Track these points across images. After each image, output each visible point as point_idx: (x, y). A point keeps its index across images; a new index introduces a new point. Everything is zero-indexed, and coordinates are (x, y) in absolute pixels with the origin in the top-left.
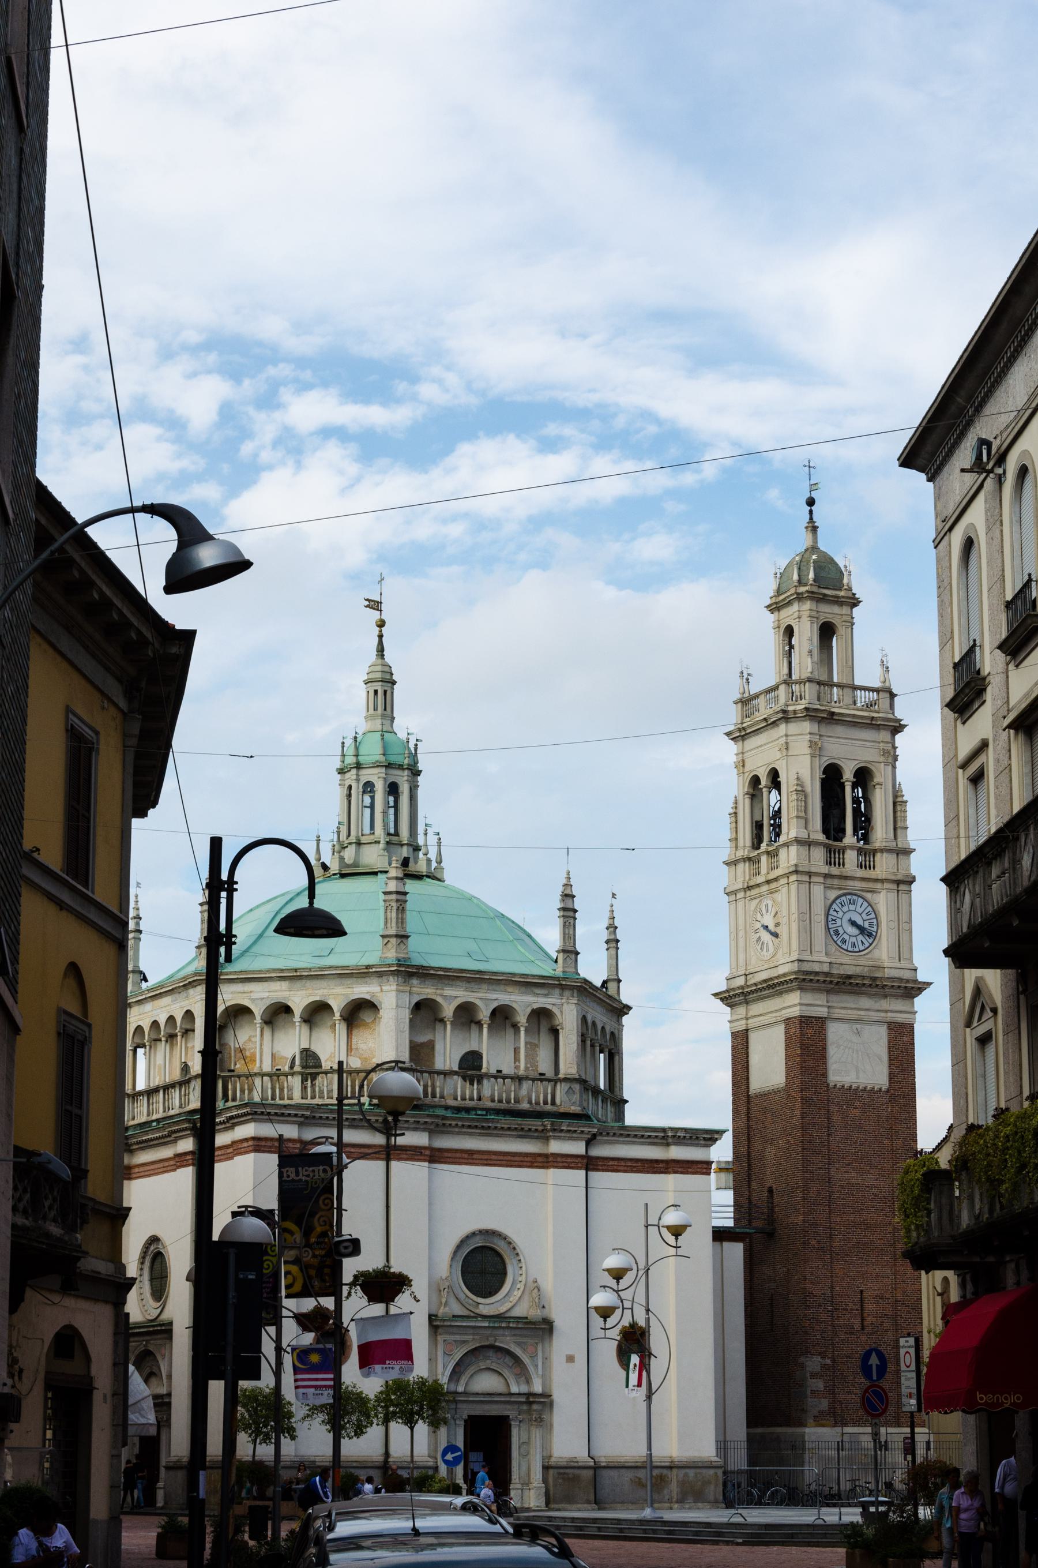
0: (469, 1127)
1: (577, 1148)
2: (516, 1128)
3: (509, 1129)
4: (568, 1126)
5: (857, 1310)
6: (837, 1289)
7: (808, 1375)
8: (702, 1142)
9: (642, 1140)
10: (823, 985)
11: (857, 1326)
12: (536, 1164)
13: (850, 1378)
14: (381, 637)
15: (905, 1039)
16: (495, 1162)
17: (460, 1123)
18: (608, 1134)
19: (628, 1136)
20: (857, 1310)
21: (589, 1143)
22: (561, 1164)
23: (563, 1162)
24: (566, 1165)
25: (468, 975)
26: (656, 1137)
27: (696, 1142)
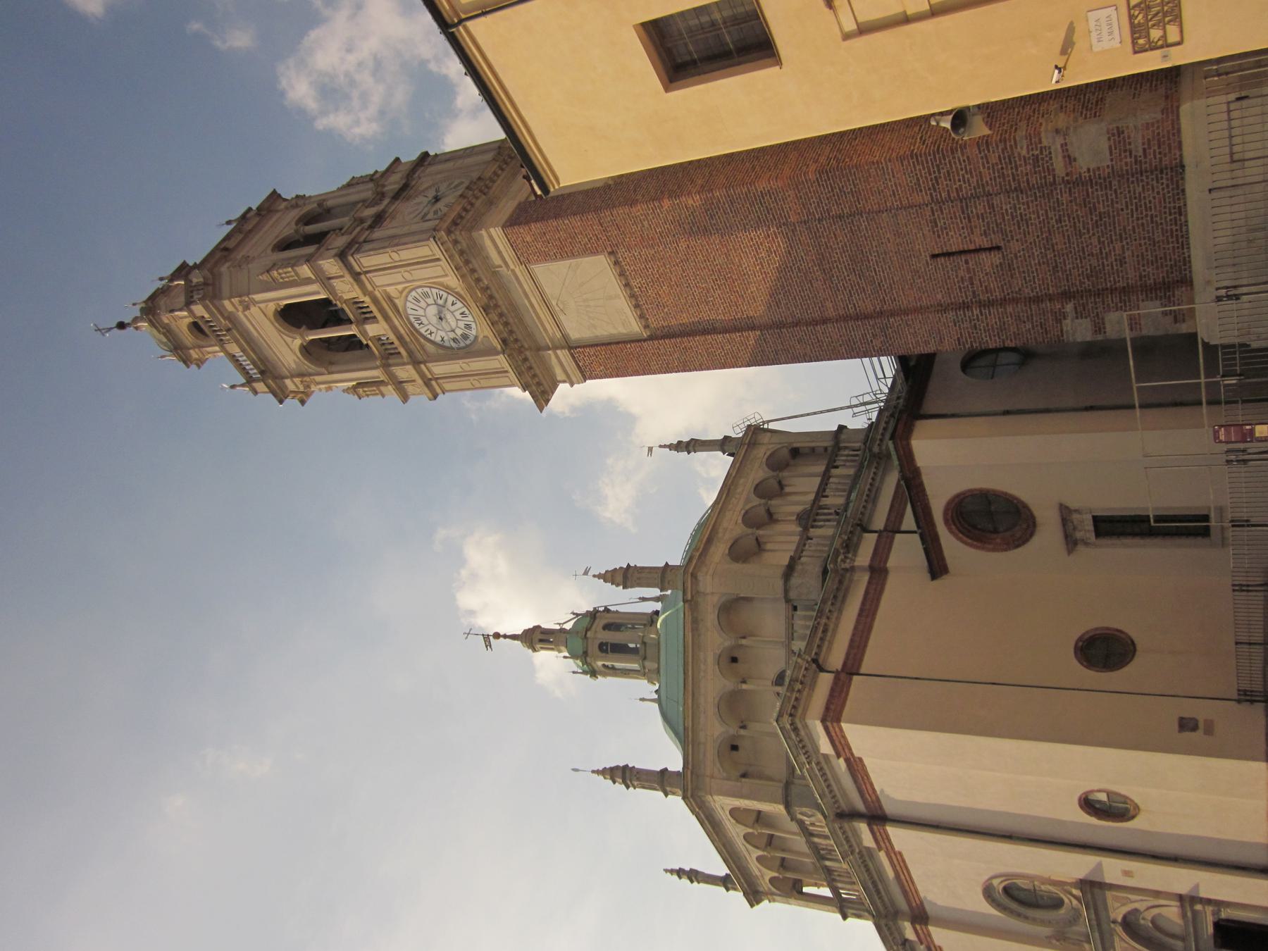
0: (878, 892)
2: (866, 866)
4: (842, 845)
5: (967, 262)
6: (939, 296)
7: (1100, 337)
8: (802, 733)
9: (828, 772)
10: (534, 365)
11: (996, 258)
13: (1094, 262)
14: (505, 636)
15: (528, 239)
19: (828, 786)
20: (967, 262)
23: (884, 843)
27: (806, 739)
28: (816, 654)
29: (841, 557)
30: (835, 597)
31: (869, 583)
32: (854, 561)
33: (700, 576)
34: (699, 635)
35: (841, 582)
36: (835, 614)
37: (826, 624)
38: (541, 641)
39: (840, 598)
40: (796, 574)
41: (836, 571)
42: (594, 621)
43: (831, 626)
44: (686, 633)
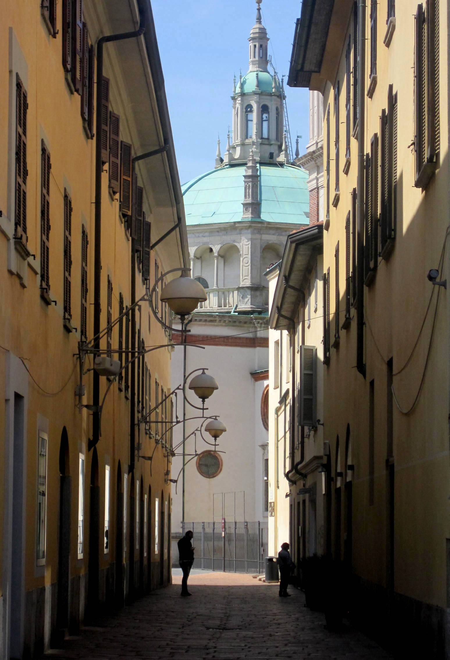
14: (259, 10)
28: (196, 320)
29: (261, 321)
30: (235, 322)
31: (247, 338)
32: (261, 327)
33: (249, 231)
34: (218, 232)
35: (245, 323)
36: (224, 324)
37: (216, 320)
38: (255, 46)
39: (234, 324)
40: (253, 292)
41: (251, 319)
42: (268, 95)
43: (216, 324)
44: (217, 225)
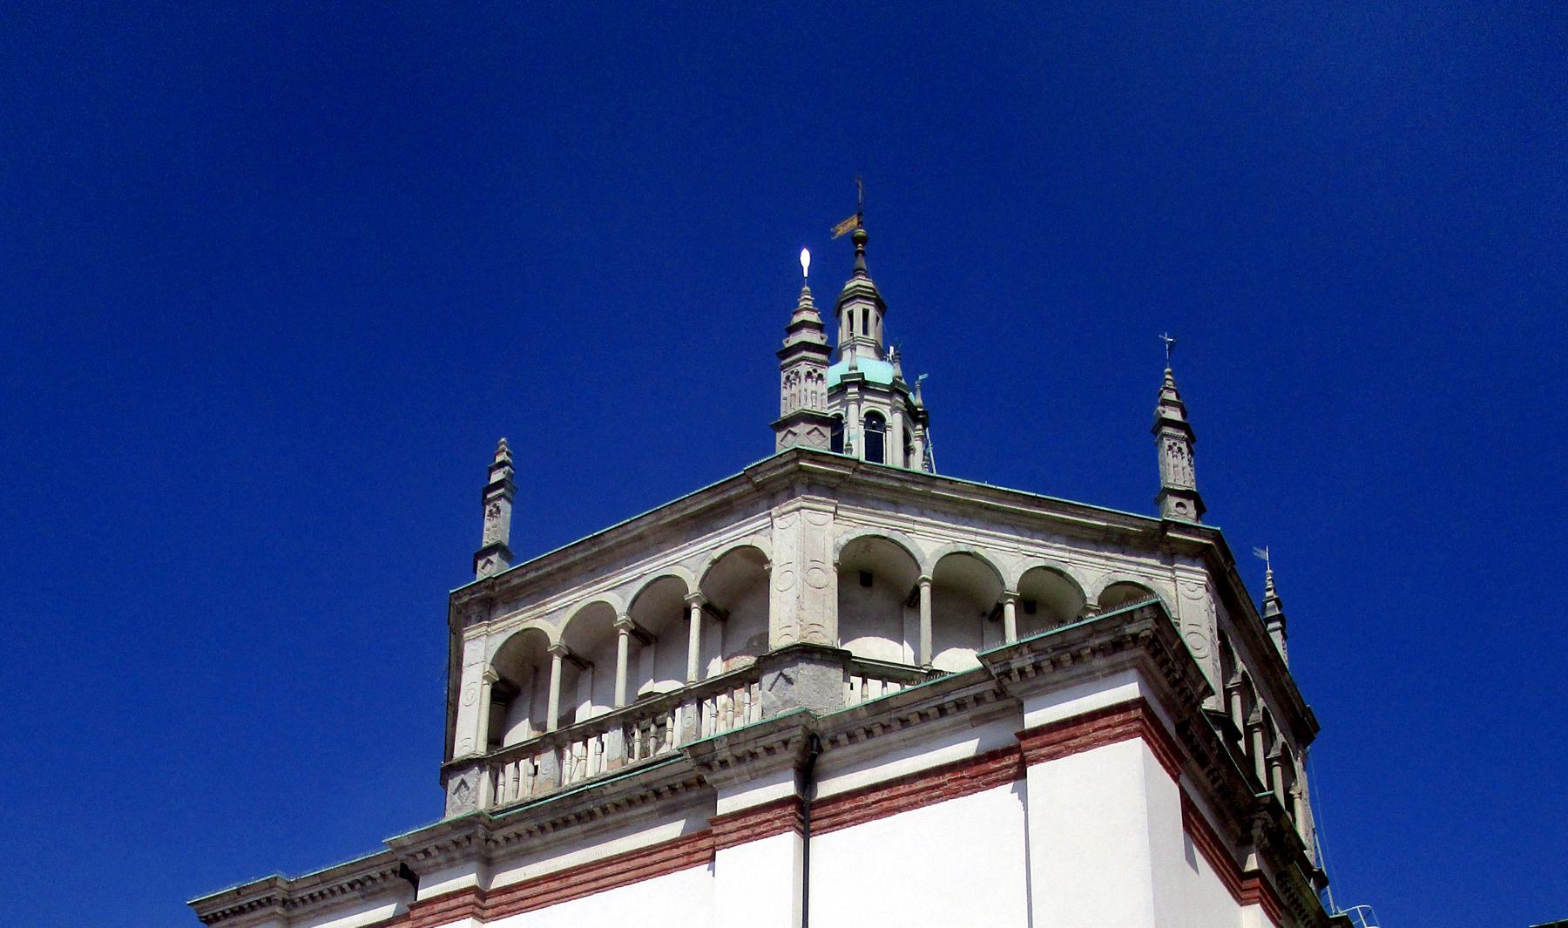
0: (555, 826)
1: (787, 788)
2: (644, 798)
3: (630, 803)
9: (946, 721)
12: (697, 857)
16: (612, 879)
17: (532, 824)
18: (852, 737)
19: (904, 722)
21: (807, 775)
22: (734, 836)
23: (738, 830)
24: (746, 832)
25: (578, 556)
26: (978, 699)
